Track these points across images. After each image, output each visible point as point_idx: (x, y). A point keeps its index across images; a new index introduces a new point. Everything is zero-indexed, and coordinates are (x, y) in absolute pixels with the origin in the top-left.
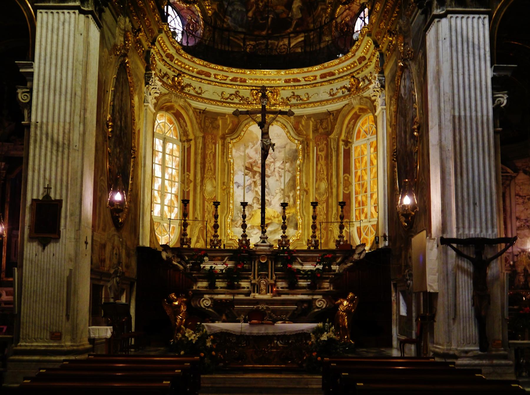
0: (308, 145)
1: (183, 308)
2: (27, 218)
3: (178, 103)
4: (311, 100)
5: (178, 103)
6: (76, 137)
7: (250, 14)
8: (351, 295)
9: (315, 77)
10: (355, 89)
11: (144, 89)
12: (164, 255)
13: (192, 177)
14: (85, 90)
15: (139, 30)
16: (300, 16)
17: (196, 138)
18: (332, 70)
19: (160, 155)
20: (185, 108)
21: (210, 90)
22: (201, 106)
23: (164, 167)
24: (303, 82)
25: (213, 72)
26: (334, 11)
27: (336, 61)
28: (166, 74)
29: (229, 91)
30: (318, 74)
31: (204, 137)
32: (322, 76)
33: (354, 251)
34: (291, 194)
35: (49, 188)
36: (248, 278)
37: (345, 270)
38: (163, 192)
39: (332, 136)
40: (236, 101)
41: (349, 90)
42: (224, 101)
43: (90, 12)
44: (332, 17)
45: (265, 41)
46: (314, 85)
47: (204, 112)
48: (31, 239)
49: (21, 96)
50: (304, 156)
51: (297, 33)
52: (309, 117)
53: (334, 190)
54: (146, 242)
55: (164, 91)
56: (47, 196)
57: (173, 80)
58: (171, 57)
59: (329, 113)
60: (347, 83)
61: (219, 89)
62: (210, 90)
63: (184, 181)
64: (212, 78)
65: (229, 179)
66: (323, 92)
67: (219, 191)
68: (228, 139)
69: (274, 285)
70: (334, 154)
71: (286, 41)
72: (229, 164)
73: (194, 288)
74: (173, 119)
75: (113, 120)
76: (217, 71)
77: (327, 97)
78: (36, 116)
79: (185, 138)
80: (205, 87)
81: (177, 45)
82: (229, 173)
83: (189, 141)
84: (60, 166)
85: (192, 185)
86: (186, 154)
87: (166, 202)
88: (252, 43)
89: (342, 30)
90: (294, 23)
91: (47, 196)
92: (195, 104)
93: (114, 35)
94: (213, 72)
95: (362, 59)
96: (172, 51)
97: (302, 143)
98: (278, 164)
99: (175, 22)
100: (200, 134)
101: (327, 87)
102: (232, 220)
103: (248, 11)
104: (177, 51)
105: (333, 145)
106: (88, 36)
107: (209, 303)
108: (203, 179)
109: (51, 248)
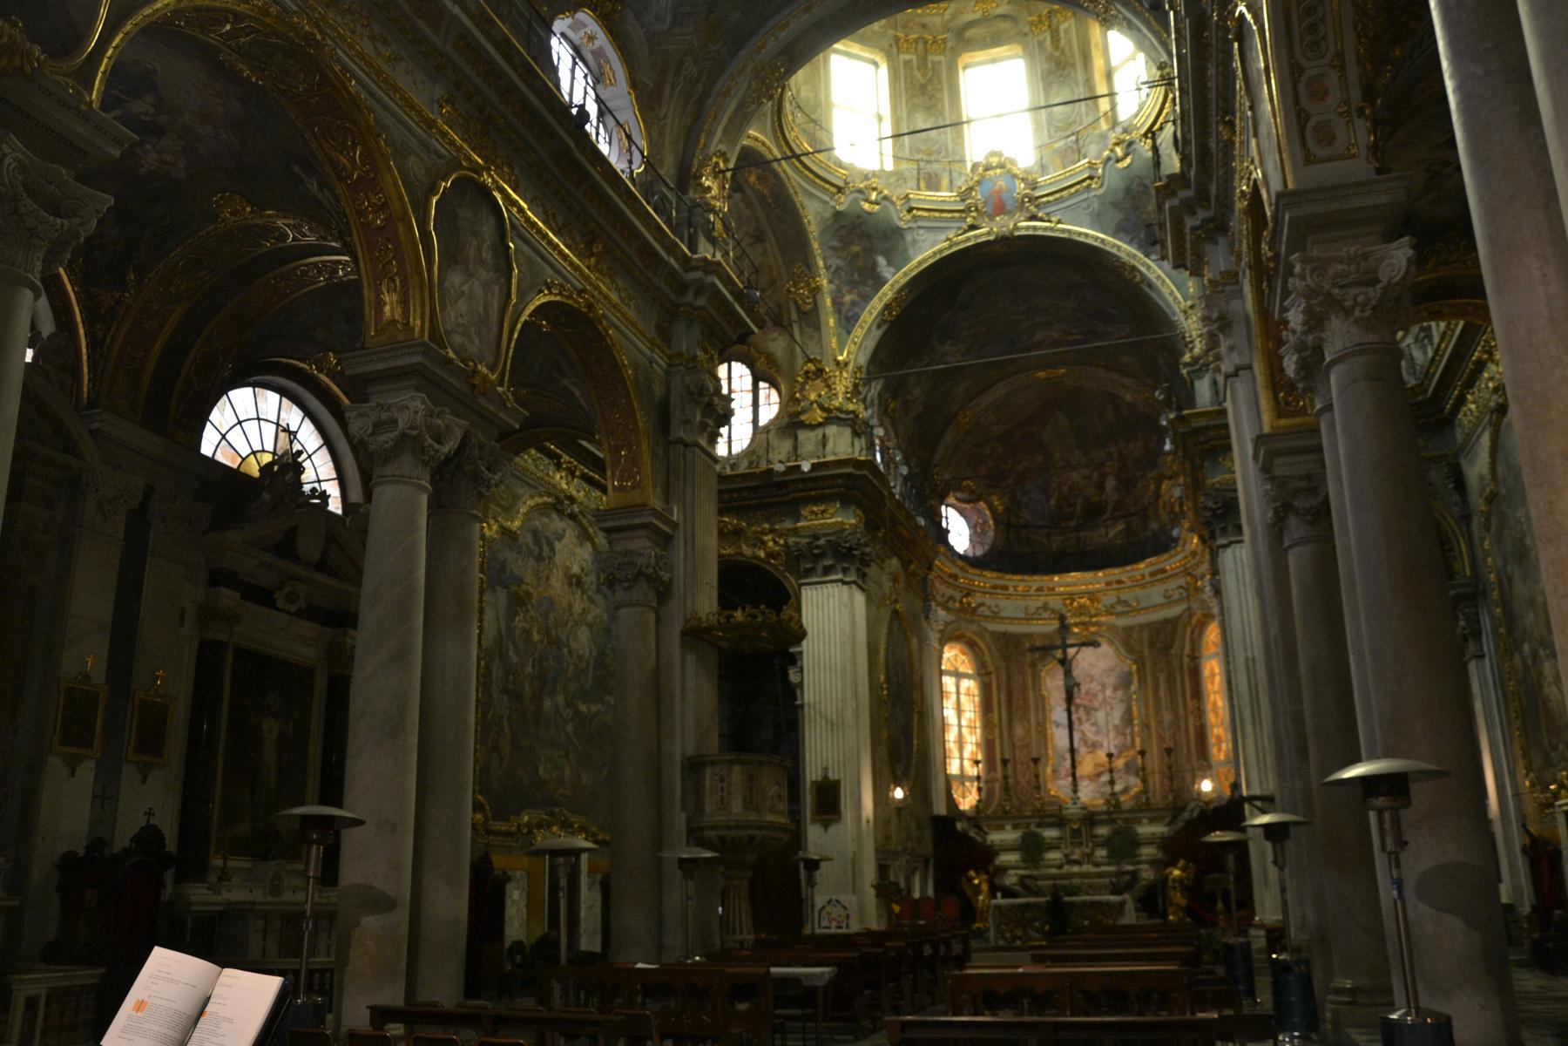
0: (1143, 665)
1: (985, 887)
2: (808, 799)
3: (970, 630)
4: (1143, 605)
5: (970, 630)
6: (849, 713)
7: (1053, 502)
8: (1181, 863)
9: (1143, 576)
10: (1192, 590)
11: (925, 625)
12: (959, 826)
13: (996, 721)
14: (855, 664)
15: (910, 562)
16: (1116, 497)
17: (998, 669)
18: (1161, 566)
19: (953, 697)
20: (980, 635)
21: (1009, 607)
22: (1000, 628)
23: (959, 710)
24: (1129, 583)
25: (1011, 584)
26: (1158, 487)
27: (1166, 556)
28: (951, 598)
29: (1034, 604)
30: (1147, 572)
31: (1007, 668)
32: (1153, 574)
33: (1183, 809)
34: (1128, 731)
35: (826, 769)
36: (1058, 848)
37: (1178, 833)
38: (961, 742)
39: (1173, 651)
40: (1045, 615)
41: (1187, 590)
42: (1029, 618)
43: (854, 582)
44: (1157, 496)
45: (1073, 535)
46: (1143, 586)
47: (1005, 635)
48: (813, 821)
49: (793, 676)
50: (1139, 682)
51: (1115, 519)
52: (1142, 627)
53: (1182, 723)
54: (941, 809)
55: (950, 618)
56: (826, 777)
57: (961, 602)
58: (955, 577)
59: (1166, 621)
60: (1182, 581)
61: (1021, 603)
62: (1009, 607)
63: (987, 725)
64: (1011, 590)
65: (1045, 717)
66: (1156, 594)
67: (1033, 734)
68: (1040, 666)
69: (1092, 854)
70: (1177, 674)
71: (1103, 531)
72: (1043, 698)
73: (997, 862)
74: (966, 649)
75: (888, 680)
76: (1019, 583)
77: (1161, 600)
78: (809, 695)
79: (983, 675)
80: (1004, 603)
81: (960, 563)
82: (1044, 709)
83: (988, 674)
84: (835, 741)
85: (997, 730)
86: (986, 690)
87: (967, 754)
88: (1060, 538)
89: (1172, 509)
90: (1110, 507)
91: (826, 777)
92: (992, 627)
93: (880, 586)
94: (1011, 584)
95: (1194, 554)
96: (956, 571)
97: (1136, 662)
98: (1108, 692)
99: (959, 532)
100: (1002, 664)
101: (1160, 588)
102: (1054, 771)
103: (1048, 499)
104: (962, 569)
105: (1175, 664)
106: (852, 608)
107: (1014, 880)
108: (1010, 721)
109: (833, 829)
